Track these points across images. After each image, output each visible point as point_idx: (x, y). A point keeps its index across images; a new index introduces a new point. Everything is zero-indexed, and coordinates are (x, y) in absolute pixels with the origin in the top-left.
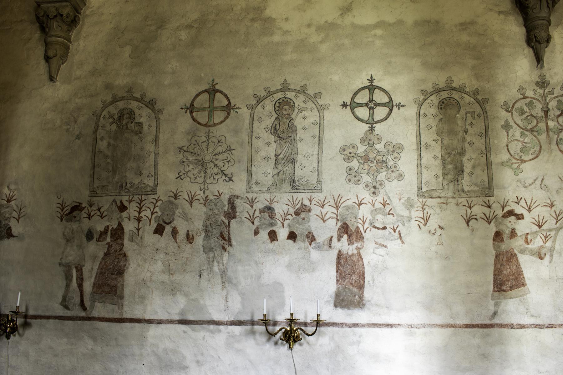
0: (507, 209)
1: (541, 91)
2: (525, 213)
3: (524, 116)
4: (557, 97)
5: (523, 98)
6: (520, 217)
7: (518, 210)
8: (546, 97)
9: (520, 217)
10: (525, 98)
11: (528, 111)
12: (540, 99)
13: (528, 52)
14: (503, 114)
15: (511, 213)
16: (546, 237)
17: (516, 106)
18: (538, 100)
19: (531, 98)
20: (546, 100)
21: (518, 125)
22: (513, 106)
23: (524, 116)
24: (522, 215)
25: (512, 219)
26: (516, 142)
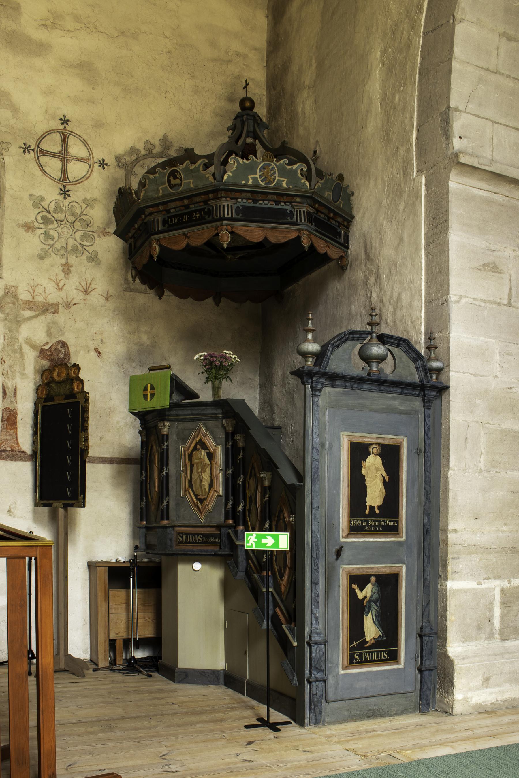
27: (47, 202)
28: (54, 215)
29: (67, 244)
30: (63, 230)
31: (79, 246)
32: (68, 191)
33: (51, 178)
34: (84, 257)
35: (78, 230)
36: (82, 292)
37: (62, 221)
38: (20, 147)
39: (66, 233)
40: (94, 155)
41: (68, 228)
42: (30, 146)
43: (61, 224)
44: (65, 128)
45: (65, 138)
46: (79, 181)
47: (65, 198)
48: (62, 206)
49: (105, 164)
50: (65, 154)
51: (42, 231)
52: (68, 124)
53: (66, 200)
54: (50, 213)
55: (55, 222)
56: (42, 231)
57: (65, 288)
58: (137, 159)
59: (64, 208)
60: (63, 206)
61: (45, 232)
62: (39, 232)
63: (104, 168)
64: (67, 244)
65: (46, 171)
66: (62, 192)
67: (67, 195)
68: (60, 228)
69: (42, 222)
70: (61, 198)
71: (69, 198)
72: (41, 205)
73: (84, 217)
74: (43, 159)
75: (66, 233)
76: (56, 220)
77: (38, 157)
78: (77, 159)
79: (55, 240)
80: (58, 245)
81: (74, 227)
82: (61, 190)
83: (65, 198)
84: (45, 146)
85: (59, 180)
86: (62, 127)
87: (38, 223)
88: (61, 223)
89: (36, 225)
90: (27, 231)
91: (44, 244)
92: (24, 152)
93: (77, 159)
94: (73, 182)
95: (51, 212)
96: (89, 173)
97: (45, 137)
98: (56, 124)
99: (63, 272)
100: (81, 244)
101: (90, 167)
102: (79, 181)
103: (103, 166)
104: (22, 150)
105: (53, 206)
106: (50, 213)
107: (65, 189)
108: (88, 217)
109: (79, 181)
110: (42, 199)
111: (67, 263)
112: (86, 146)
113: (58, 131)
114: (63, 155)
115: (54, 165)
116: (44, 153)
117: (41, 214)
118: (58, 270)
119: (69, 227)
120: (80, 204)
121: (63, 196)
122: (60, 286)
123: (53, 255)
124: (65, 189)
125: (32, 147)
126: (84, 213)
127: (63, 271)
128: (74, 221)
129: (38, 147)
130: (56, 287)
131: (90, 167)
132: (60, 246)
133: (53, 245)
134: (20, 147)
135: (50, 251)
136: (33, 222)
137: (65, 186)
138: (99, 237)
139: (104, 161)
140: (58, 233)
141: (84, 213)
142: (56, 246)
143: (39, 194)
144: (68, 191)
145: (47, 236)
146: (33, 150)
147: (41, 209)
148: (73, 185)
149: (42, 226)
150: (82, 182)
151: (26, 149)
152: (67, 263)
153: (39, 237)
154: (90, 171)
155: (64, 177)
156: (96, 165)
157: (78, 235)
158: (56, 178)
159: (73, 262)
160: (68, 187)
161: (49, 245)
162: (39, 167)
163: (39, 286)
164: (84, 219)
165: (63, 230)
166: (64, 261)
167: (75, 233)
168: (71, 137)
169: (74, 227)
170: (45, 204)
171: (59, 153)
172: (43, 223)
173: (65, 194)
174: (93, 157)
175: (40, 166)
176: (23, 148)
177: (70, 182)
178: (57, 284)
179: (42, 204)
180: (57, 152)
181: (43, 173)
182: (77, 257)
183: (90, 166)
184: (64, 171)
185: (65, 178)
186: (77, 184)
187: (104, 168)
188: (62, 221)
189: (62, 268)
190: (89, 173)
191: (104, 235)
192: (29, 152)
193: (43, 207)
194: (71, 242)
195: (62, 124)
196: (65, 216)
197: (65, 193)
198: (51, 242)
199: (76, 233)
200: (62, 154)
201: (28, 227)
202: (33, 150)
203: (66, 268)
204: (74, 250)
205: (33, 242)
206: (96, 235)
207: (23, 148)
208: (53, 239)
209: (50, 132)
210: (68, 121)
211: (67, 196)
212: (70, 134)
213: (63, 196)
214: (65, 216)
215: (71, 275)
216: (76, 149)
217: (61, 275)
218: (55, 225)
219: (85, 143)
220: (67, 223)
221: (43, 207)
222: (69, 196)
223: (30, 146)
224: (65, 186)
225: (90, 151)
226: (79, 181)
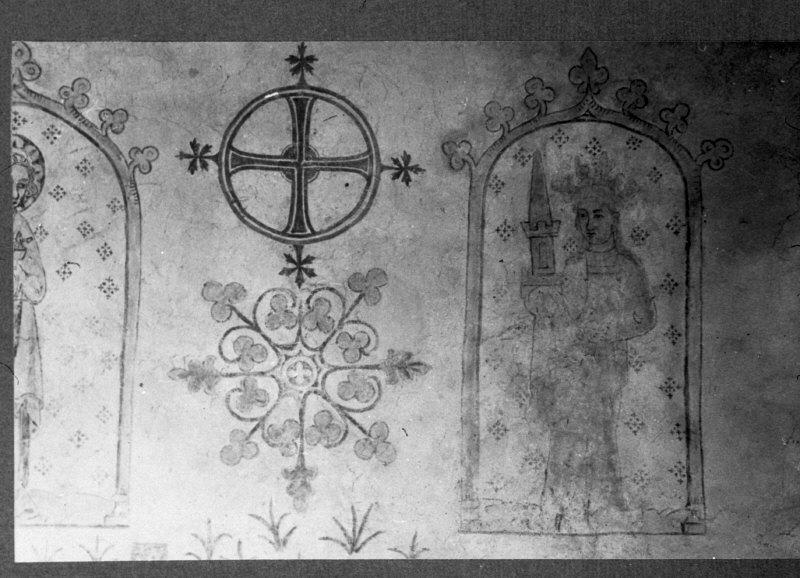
27: (250, 301)
28: (269, 333)
29: (301, 413)
30: (293, 374)
31: (335, 412)
32: (309, 260)
33: (261, 228)
34: (349, 444)
35: (336, 368)
36: (343, 545)
37: (290, 347)
38: (182, 156)
39: (300, 380)
40: (381, 147)
41: (306, 366)
42: (207, 148)
43: (287, 358)
44: (302, 84)
45: (301, 112)
46: (339, 229)
47: (299, 281)
48: (290, 304)
49: (412, 169)
50: (301, 155)
51: (235, 382)
52: (310, 69)
53: (304, 286)
54: (257, 328)
55: (271, 352)
56: (235, 382)
57: (292, 539)
58: (502, 138)
59: (296, 311)
60: (294, 305)
61: (244, 383)
62: (226, 385)
63: (407, 180)
64: (301, 413)
65: (248, 211)
66: (291, 266)
67: (306, 270)
68: (285, 367)
69: (236, 356)
71: (313, 280)
72: (233, 309)
73: (350, 329)
74: (244, 181)
75: (300, 380)
76: (275, 347)
77: (229, 175)
78: (335, 165)
79: (269, 406)
81: (323, 361)
82: (289, 259)
83: (299, 281)
84: (250, 141)
85: (284, 233)
86: (294, 81)
87: (225, 359)
88: (290, 353)
89: (219, 365)
90: (195, 387)
91: (239, 418)
92: (192, 168)
93: (335, 165)
94: (320, 233)
95: (262, 326)
96: (367, 200)
97: (249, 115)
99: (291, 494)
100: (341, 408)
101: (368, 185)
102: (339, 229)
103: (407, 175)
104: (187, 162)
105: (264, 308)
106: (257, 328)
107: (299, 256)
108: (361, 327)
109: (338, 228)
110: (239, 291)
111: (301, 468)
112: (358, 123)
114: (298, 164)
115: (266, 193)
116: (246, 162)
117: (234, 335)
118: (276, 492)
119: (309, 361)
120: (343, 292)
121: (294, 276)
122: (282, 535)
123: (264, 447)
124: (299, 256)
125: (214, 151)
126: (352, 317)
127: (290, 490)
128: (325, 344)
129: (230, 146)
130: (272, 537)
131: (368, 185)
132: (283, 419)
133: (263, 419)
134: (182, 156)
135: (257, 437)
136: (211, 359)
137: (299, 248)
138: (392, 381)
139: (407, 158)
140: (278, 381)
141: (352, 317)
142: (270, 421)
143: (230, 280)
144: (309, 260)
145: (251, 396)
146: (216, 158)
147: (235, 321)
148: (321, 239)
149: (235, 368)
150: (347, 228)
151: (196, 158)
152: (301, 468)
153: (227, 400)
154: (369, 194)
155: (299, 220)
156: (386, 176)
157: (333, 383)
158: (275, 227)
159: (319, 464)
160: (309, 250)
161: (252, 420)
162: (231, 204)
163: (225, 539)
164: (352, 333)
165: (293, 374)
166: (291, 463)
167: (325, 377)
168: (319, 104)
169: (323, 361)
170: (245, 306)
171: (288, 153)
172: (238, 359)
173: (300, 269)
174: (378, 154)
175: (233, 200)
176: (189, 156)
177: (314, 233)
178: (274, 529)
179: (238, 305)
180: (279, 153)
181: (241, 219)
182: (328, 447)
183: (368, 179)
184: (299, 202)
185: (303, 224)
186: (333, 236)
187: (407, 180)
188: (290, 347)
189: (287, 483)
190: (367, 200)
191: (407, 374)
192: (205, 166)
193: (240, 315)
194: (314, 404)
195: (295, 71)
196: (299, 333)
197: (299, 267)
198: (258, 412)
199: (329, 376)
200: (294, 157)
201: (198, 377)
202: (216, 158)
203: (299, 482)
206: (382, 376)
207: (189, 156)
208: (263, 403)
209: (259, 101)
210: (312, 59)
211: (305, 276)
212: (316, 97)
213: (294, 276)
214: (299, 333)
215: (311, 499)
216: (331, 135)
217: (283, 503)
218: (272, 359)
219: (357, 116)
220: (304, 349)
221: (240, 315)
222: (312, 274)
223: (207, 148)
224: (299, 248)
225: (369, 137)
226: (338, 228)
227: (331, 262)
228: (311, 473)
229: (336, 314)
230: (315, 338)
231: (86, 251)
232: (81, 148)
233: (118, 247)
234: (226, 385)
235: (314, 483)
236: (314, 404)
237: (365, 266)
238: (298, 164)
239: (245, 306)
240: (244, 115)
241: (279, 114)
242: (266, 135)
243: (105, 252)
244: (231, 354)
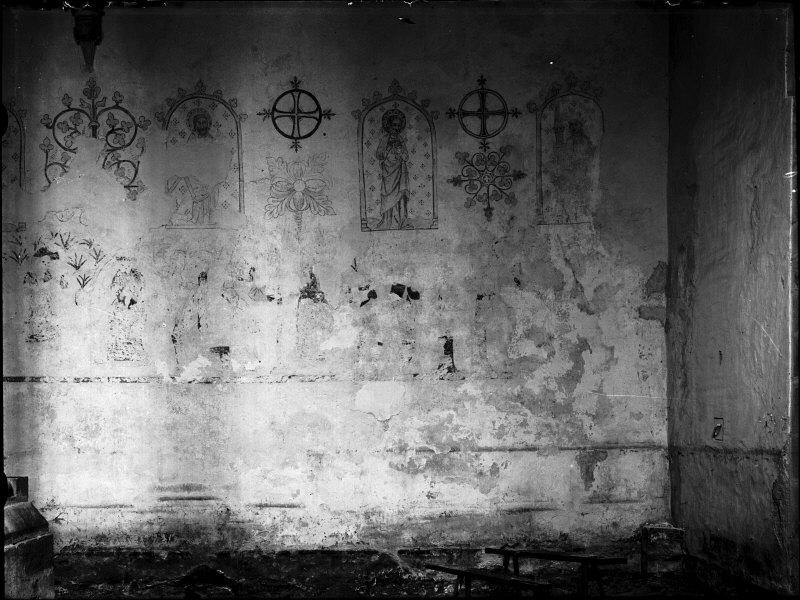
0: (39, 247)
1: (89, 102)
2: (61, 251)
3: (68, 133)
4: (109, 109)
5: (68, 111)
6: (55, 256)
7: (53, 248)
8: (94, 108)
9: (55, 256)
10: (70, 109)
11: (73, 126)
12: (87, 110)
13: (78, 49)
14: (44, 132)
15: (43, 252)
16: (84, 280)
17: (59, 120)
18: (84, 112)
19: (76, 110)
20: (94, 113)
21: (60, 144)
22: (55, 121)
23: (68, 133)
24: (56, 253)
25: (46, 258)
26: (57, 166)
70: (482, 151)
78: (494, 113)
80: (481, 193)
90: (455, 185)
98: (475, 86)
109: (497, 133)
113: (477, 91)
115: (474, 124)
116: (466, 114)
138: (515, 179)
146: (457, 113)
157: (497, 181)
170: (469, 159)
171: (479, 110)
197: (485, 146)
201: (456, 182)
202: (457, 113)
204: (497, 197)
205: (460, 195)
206: (512, 178)
209: (470, 94)
216: (493, 103)
219: (501, 98)
225: (505, 104)
226: (497, 133)
227: (495, 144)
228: (492, 209)
229: (497, 160)
230: (492, 168)
231: (420, 144)
232: (416, 112)
233: (429, 143)
234: (464, 184)
235: (493, 212)
236: (492, 188)
237: (505, 145)
238: (483, 114)
239: (469, 159)
240: (465, 99)
241: (476, 98)
242: (472, 105)
243: (426, 145)
244: (465, 173)
